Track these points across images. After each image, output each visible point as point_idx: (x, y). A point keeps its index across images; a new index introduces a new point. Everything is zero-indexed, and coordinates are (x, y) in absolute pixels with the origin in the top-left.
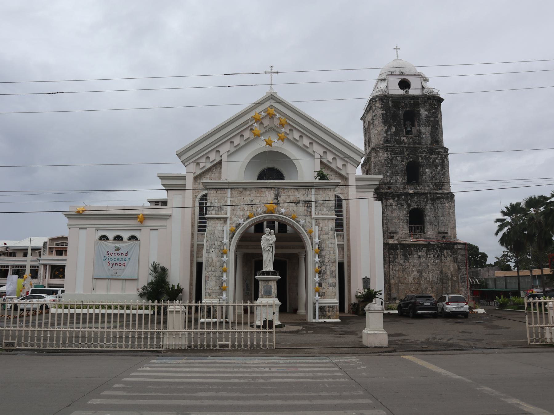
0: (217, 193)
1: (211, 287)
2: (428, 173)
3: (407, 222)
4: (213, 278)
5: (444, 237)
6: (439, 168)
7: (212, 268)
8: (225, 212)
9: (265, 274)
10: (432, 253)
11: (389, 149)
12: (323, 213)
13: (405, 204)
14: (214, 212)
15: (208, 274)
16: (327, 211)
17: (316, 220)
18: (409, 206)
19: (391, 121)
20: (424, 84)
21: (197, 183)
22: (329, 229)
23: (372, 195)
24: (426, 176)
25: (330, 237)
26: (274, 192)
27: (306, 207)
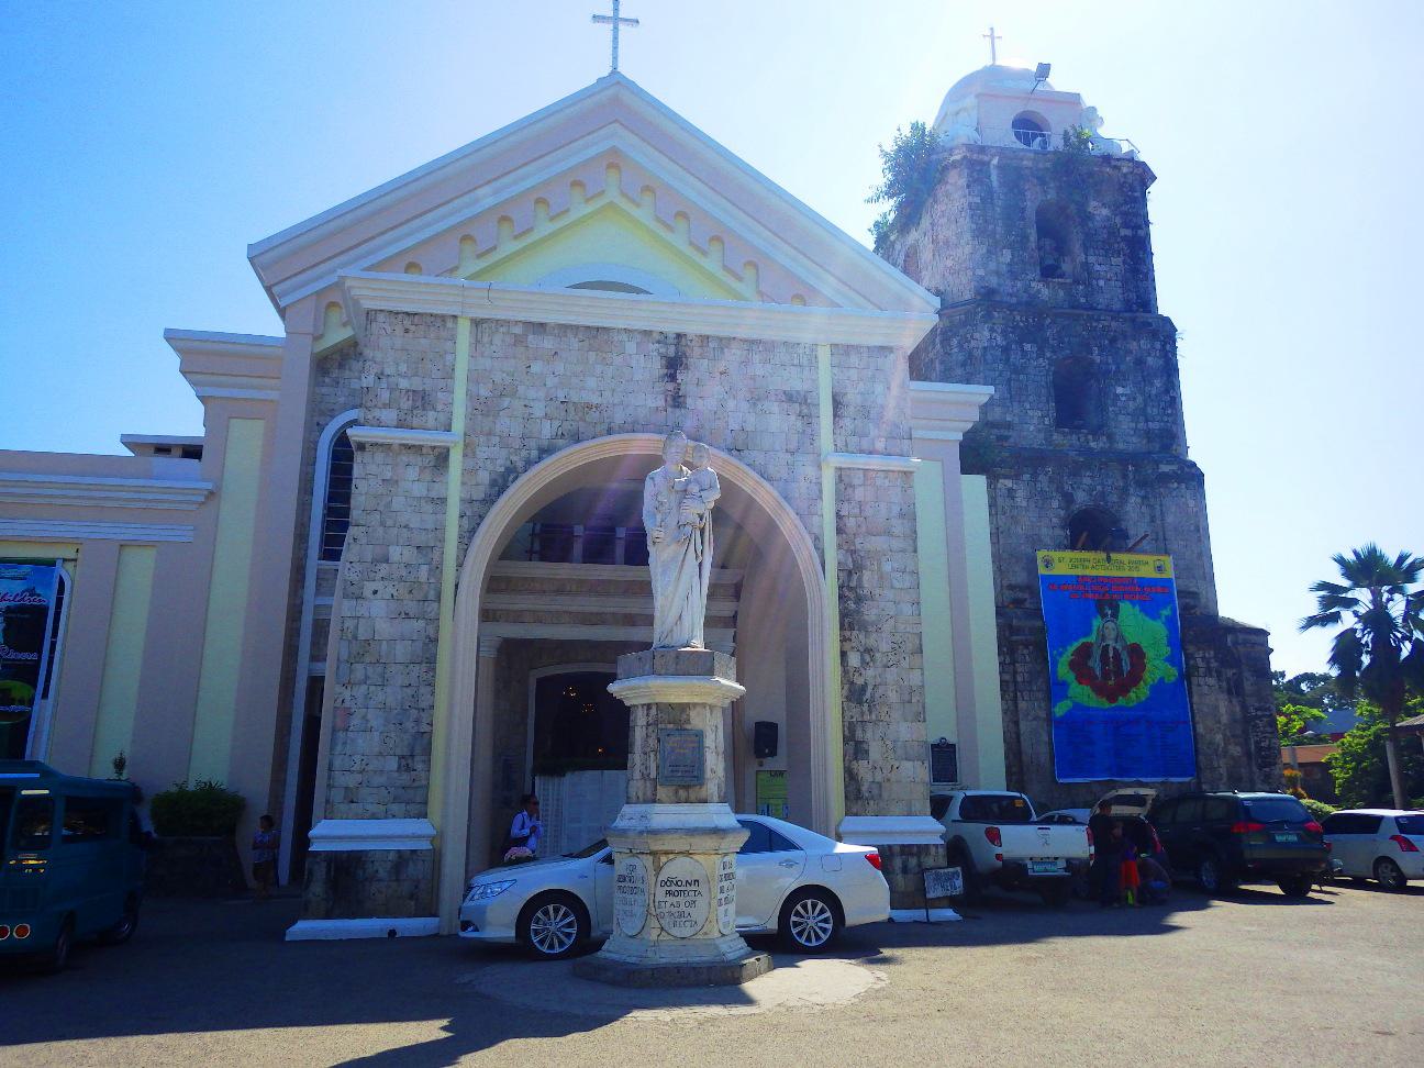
0: (410, 335)
1: (357, 758)
2: (1123, 399)
4: (369, 716)
6: (1158, 383)
8: (442, 417)
14: (389, 416)
15: (347, 694)
18: (1068, 499)
19: (999, 229)
25: (896, 544)
27: (793, 418)
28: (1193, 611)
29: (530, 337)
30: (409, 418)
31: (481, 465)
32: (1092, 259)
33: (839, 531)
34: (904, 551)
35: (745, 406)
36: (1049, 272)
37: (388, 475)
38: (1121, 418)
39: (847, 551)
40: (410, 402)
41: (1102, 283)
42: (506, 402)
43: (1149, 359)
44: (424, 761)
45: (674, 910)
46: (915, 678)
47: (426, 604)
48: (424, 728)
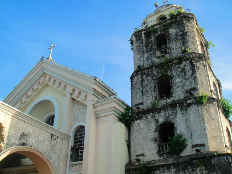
13: (153, 121)
18: (157, 121)
38: (177, 89)
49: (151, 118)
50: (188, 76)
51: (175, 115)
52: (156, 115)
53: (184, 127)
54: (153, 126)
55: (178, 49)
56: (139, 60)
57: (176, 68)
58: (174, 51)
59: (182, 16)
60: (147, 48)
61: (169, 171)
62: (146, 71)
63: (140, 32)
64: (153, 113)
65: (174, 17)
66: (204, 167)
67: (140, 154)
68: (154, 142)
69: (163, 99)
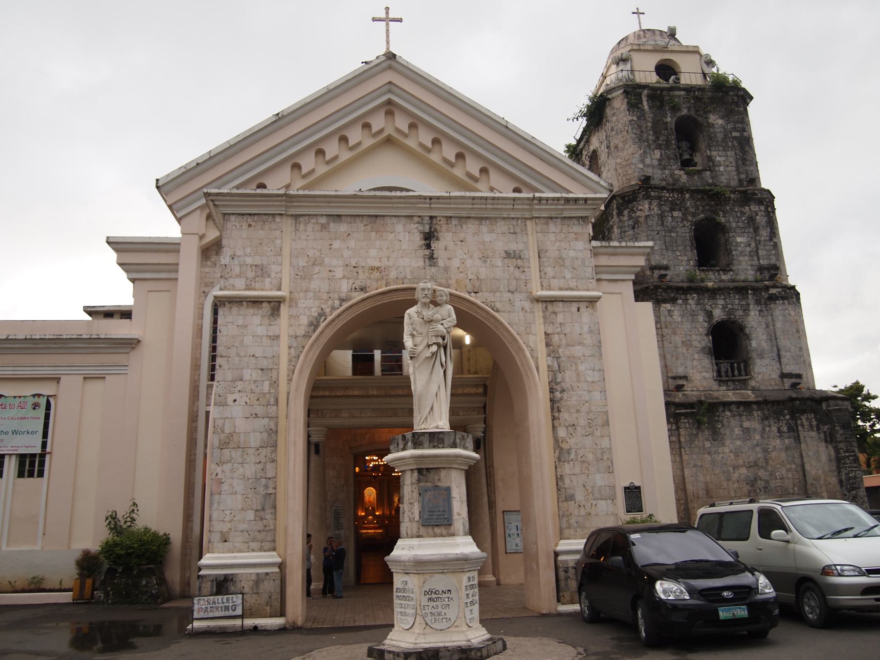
0: (252, 228)
1: (228, 512)
3: (711, 353)
4: (235, 484)
5: (794, 386)
7: (233, 452)
9: (426, 444)
10: (775, 423)
11: (653, 194)
12: (562, 283)
13: (700, 312)
15: (219, 470)
16: (572, 278)
17: (544, 305)
18: (709, 315)
19: (650, 137)
20: (707, 70)
21: (209, 263)
22: (581, 328)
23: (628, 290)
24: (737, 252)
25: (588, 352)
26: (421, 228)
27: (512, 269)
28: (798, 387)
29: (332, 225)
30: (253, 283)
31: (302, 312)
32: (714, 153)
33: (548, 345)
34: (593, 356)
35: (478, 262)
36: (686, 164)
37: (240, 322)
38: (741, 258)
39: (553, 358)
40: (253, 273)
41: (722, 169)
42: (317, 269)
43: (758, 217)
44: (271, 513)
45: (434, 611)
46: (605, 443)
47: (269, 407)
48: (271, 491)
49: (696, 305)
50: (763, 238)
51: (745, 310)
52: (707, 301)
53: (765, 337)
54: (702, 324)
55: (729, 169)
56: (643, 161)
57: (736, 212)
58: (722, 169)
59: (740, 96)
60: (658, 138)
61: (750, 415)
62: (667, 195)
63: (640, 88)
64: (698, 294)
65: (724, 89)
66: (813, 415)
67: (679, 374)
68: (706, 355)
69: (712, 271)
